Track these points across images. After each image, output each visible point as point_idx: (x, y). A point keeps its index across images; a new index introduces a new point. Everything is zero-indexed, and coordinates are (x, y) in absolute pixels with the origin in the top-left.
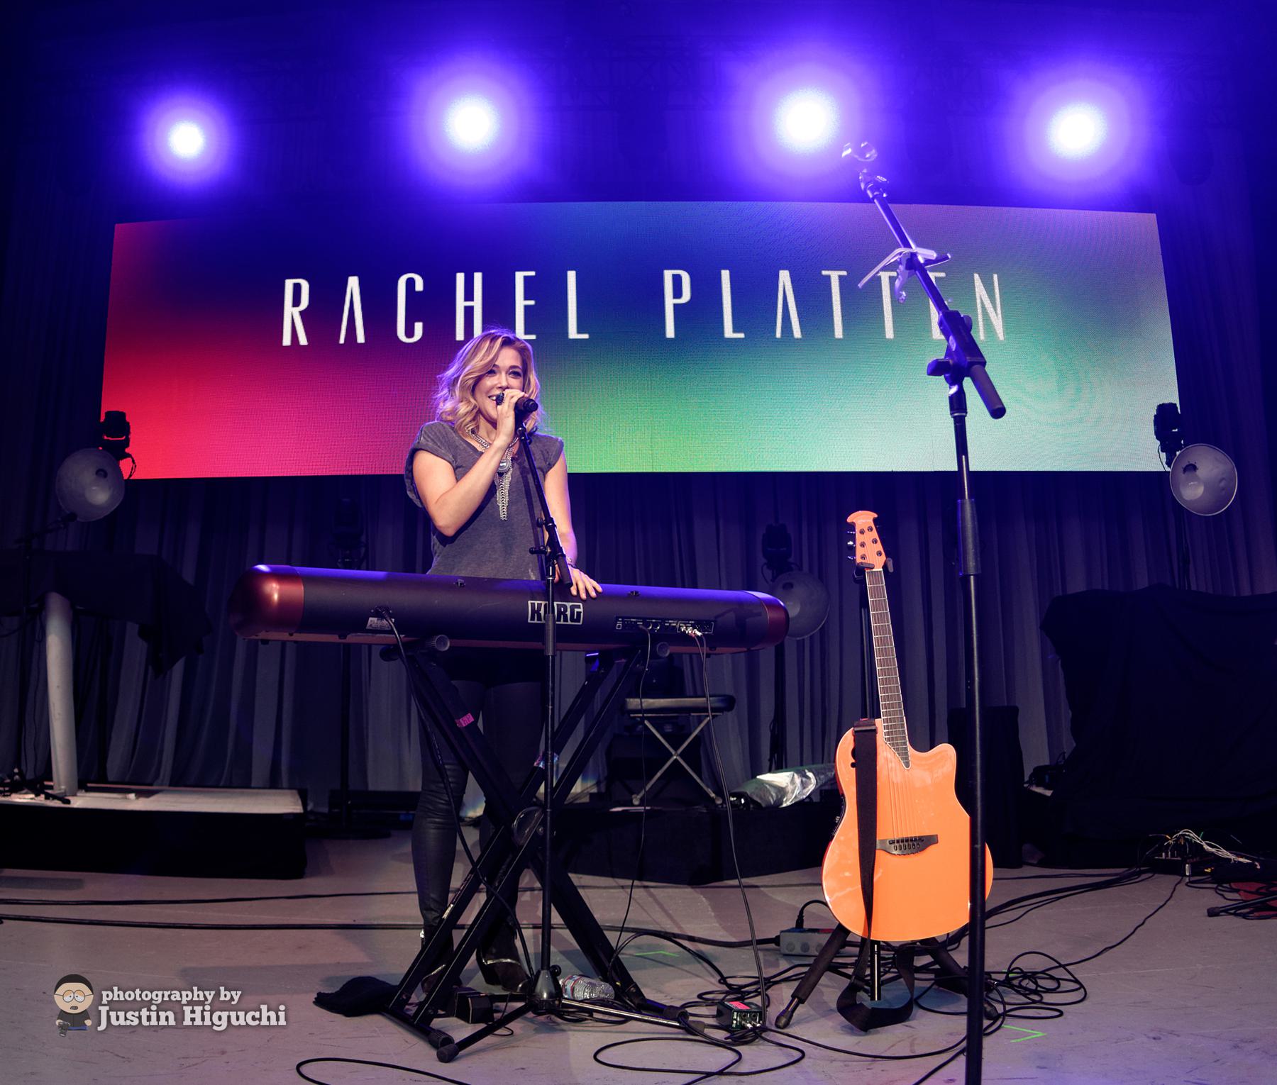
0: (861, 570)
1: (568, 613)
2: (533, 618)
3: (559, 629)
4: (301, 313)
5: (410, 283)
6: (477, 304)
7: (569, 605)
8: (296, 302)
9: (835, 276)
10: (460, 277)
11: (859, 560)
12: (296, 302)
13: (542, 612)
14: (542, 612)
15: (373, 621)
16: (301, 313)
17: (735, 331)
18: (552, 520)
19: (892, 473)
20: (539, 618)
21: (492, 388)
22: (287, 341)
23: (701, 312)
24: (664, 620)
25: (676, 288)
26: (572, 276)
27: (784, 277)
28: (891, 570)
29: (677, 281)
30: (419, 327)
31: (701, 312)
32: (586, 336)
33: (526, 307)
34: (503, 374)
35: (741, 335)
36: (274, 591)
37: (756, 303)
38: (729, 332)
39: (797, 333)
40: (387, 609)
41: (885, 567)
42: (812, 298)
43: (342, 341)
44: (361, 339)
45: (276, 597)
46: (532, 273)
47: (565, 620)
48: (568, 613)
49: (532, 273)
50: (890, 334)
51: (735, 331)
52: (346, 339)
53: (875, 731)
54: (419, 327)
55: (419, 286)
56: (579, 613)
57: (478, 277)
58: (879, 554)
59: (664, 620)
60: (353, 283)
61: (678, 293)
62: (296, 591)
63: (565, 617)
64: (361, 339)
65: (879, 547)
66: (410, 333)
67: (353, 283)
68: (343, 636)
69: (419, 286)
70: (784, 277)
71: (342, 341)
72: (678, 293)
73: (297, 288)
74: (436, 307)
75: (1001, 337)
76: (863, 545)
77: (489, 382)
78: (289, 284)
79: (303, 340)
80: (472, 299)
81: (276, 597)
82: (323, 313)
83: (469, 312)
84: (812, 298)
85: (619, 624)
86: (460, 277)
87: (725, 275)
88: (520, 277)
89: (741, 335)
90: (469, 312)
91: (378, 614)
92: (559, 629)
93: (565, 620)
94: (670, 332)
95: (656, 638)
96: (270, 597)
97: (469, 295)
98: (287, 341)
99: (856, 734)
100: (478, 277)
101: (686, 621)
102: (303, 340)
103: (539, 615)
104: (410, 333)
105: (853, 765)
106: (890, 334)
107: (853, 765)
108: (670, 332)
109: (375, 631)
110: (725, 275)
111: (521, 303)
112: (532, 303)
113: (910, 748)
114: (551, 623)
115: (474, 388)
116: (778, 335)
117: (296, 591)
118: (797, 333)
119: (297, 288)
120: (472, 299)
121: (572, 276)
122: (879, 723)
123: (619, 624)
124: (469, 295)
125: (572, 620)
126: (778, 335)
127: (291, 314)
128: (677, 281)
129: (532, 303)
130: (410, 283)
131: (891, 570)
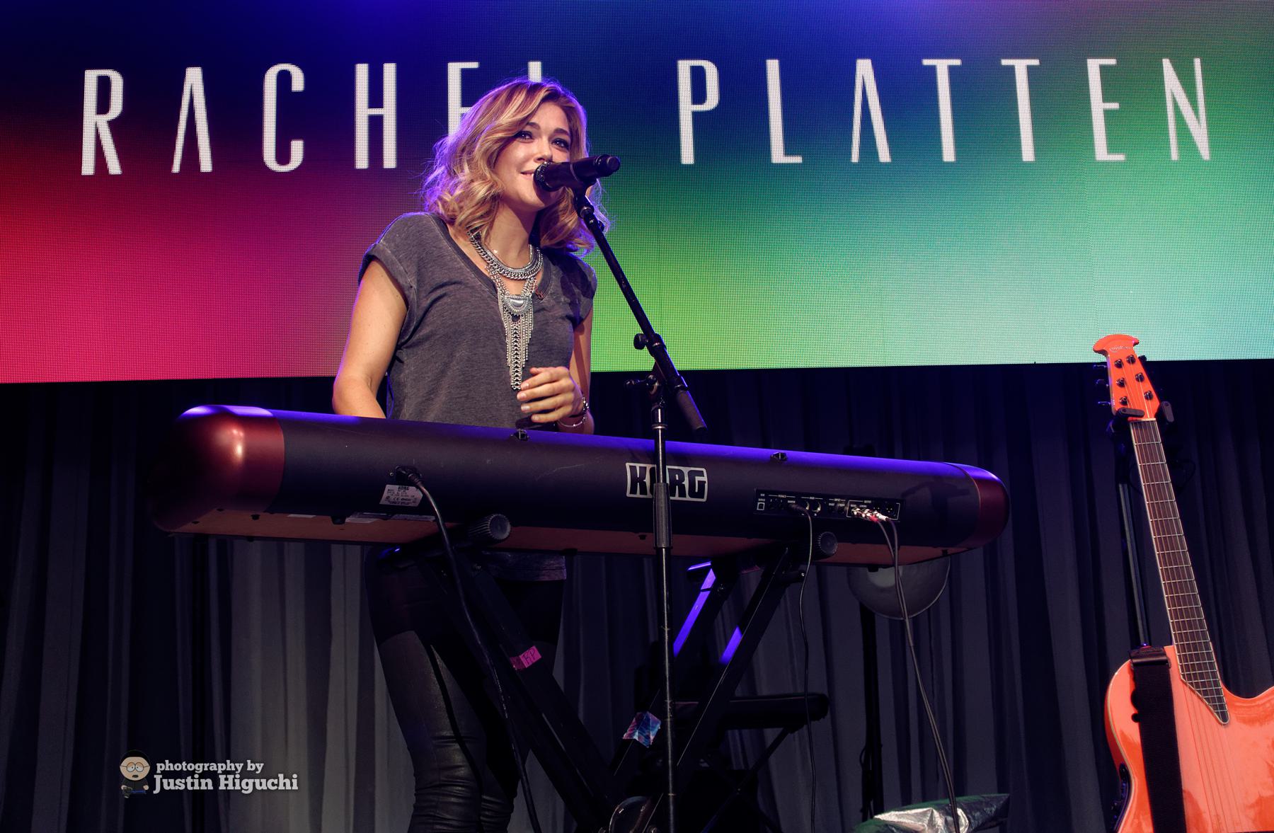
0: (1124, 420)
1: (686, 483)
2: (633, 491)
3: (674, 508)
4: (111, 124)
5: (284, 78)
6: (389, 111)
7: (686, 470)
8: (103, 107)
11: (1115, 404)
12: (103, 107)
13: (647, 480)
14: (647, 480)
15: (392, 492)
16: (111, 124)
18: (658, 338)
19: (1035, 365)
20: (643, 491)
21: (527, 160)
22: (88, 168)
23: (734, 126)
25: (696, 89)
28: (1170, 417)
29: (698, 77)
30: (297, 148)
31: (734, 126)
34: (545, 139)
35: (798, 160)
36: (236, 443)
37: (818, 108)
38: (778, 155)
39: (884, 155)
40: (414, 470)
41: (1160, 415)
42: (907, 98)
43: (176, 168)
44: (206, 165)
45: (239, 450)
47: (682, 494)
48: (686, 483)
50: (1028, 154)
51: (788, 152)
52: (182, 166)
53: (1165, 664)
54: (297, 148)
55: (298, 83)
56: (702, 484)
58: (1149, 397)
59: (827, 497)
60: (194, 78)
61: (699, 94)
62: (274, 442)
63: (682, 488)
64: (206, 165)
65: (1147, 386)
66: (283, 155)
67: (194, 78)
68: (339, 519)
69: (298, 83)
71: (176, 168)
72: (699, 94)
73: (104, 84)
74: (318, 118)
76: (1122, 384)
77: (520, 151)
78: (91, 77)
79: (114, 167)
80: (380, 105)
81: (239, 450)
82: (146, 124)
83: (376, 124)
84: (907, 98)
85: (761, 502)
89: (798, 160)
90: (376, 124)
91: (403, 481)
92: (674, 508)
93: (682, 494)
94: (687, 155)
95: (820, 524)
96: (226, 453)
97: (376, 99)
98: (88, 168)
99: (1137, 672)
101: (859, 499)
102: (114, 167)
103: (643, 485)
104: (283, 155)
105: (1135, 718)
106: (1028, 154)
107: (1135, 718)
108: (687, 155)
109: (395, 509)
114: (662, 496)
115: (495, 159)
116: (855, 158)
117: (274, 442)
118: (884, 155)
119: (104, 84)
120: (380, 105)
123: (761, 502)
124: (376, 99)
125: (692, 494)
126: (855, 158)
127: (95, 126)
128: (698, 77)
130: (284, 78)
131: (1170, 417)
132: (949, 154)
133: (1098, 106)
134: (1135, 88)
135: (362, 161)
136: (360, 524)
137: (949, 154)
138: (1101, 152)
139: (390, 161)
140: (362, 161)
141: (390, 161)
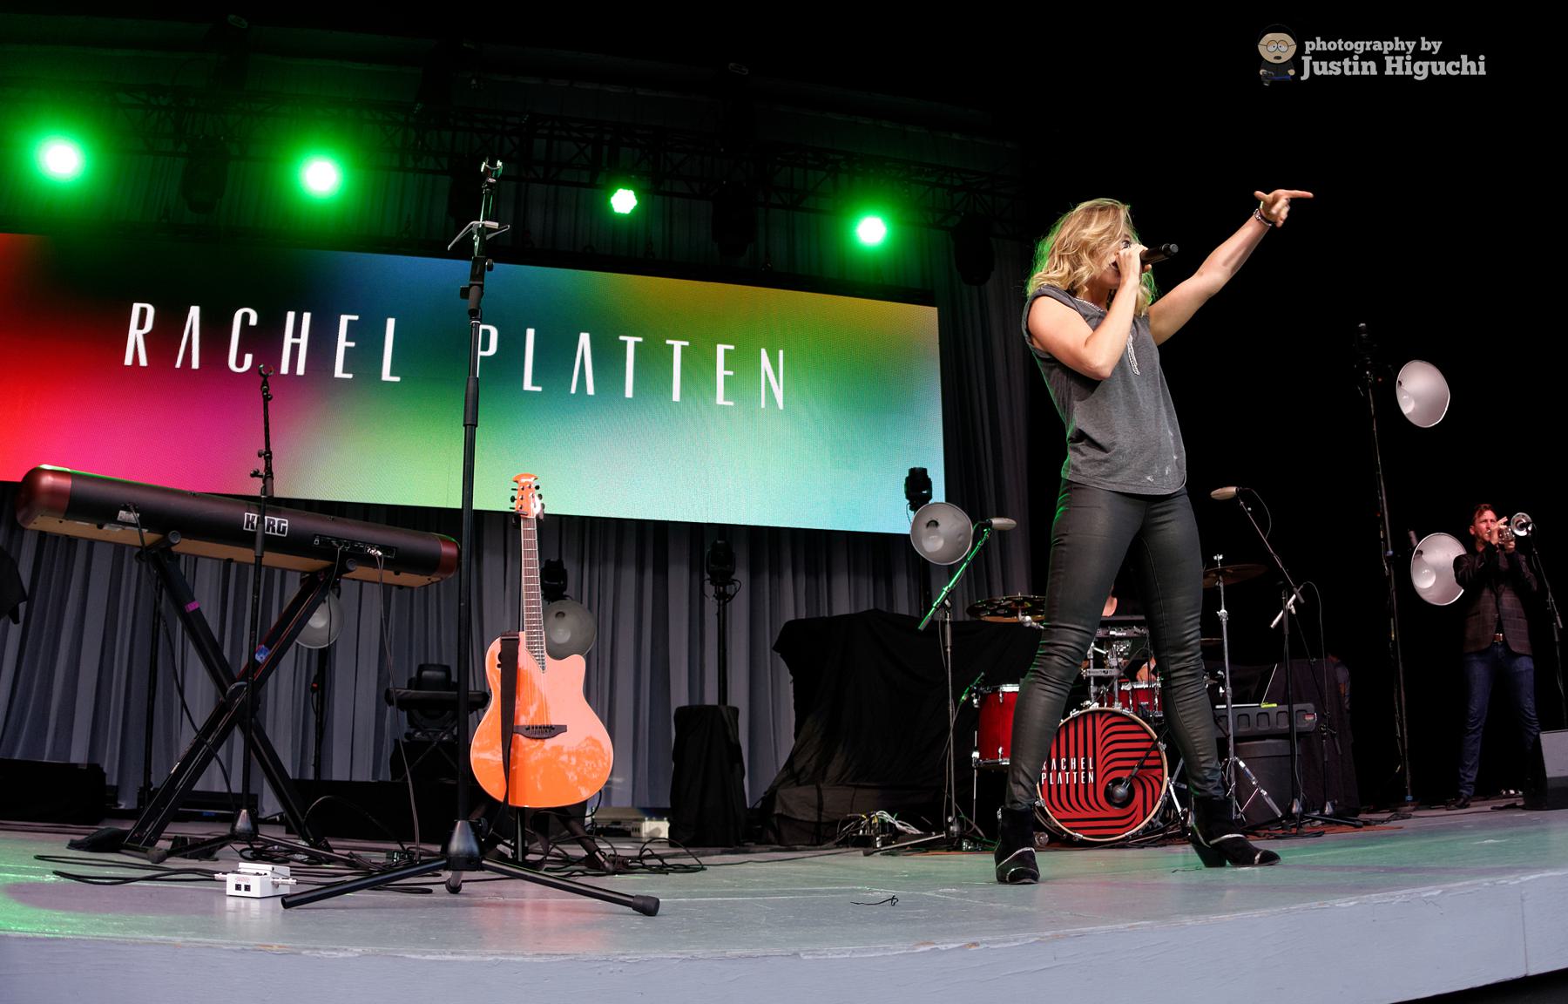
5: (246, 317)
6: (303, 342)
8: (141, 325)
9: (631, 342)
10: (291, 316)
12: (141, 325)
15: (122, 514)
16: (145, 336)
17: (534, 384)
22: (128, 361)
24: (354, 542)
26: (391, 323)
27: (585, 339)
30: (248, 358)
32: (397, 379)
33: (347, 349)
35: (539, 389)
37: (556, 359)
38: (528, 385)
39: (591, 390)
42: (609, 357)
43: (178, 365)
44: (195, 365)
46: (356, 318)
49: (356, 318)
51: (534, 384)
54: (248, 358)
55: (253, 321)
57: (307, 316)
60: (195, 312)
64: (195, 365)
66: (240, 363)
67: (195, 312)
68: (100, 527)
69: (253, 321)
70: (585, 339)
71: (178, 365)
73: (143, 312)
74: (263, 341)
75: (781, 406)
78: (137, 307)
79: (143, 362)
82: (164, 339)
83: (295, 348)
84: (609, 357)
85: (317, 540)
86: (291, 316)
87: (531, 333)
88: (344, 320)
89: (539, 389)
90: (295, 348)
91: (126, 509)
97: (297, 334)
98: (128, 361)
100: (307, 316)
102: (143, 362)
104: (240, 363)
109: (125, 524)
110: (531, 333)
111: (342, 343)
112: (352, 344)
113: (547, 657)
116: (573, 391)
118: (591, 390)
119: (143, 312)
121: (391, 323)
122: (523, 635)
123: (317, 540)
124: (297, 334)
126: (573, 391)
127: (136, 336)
129: (352, 344)
130: (246, 317)
132: (629, 393)
133: (721, 372)
134: (743, 362)
135: (284, 370)
136: (111, 532)
137: (629, 393)
138: (720, 399)
139: (301, 371)
140: (284, 370)
141: (301, 371)
